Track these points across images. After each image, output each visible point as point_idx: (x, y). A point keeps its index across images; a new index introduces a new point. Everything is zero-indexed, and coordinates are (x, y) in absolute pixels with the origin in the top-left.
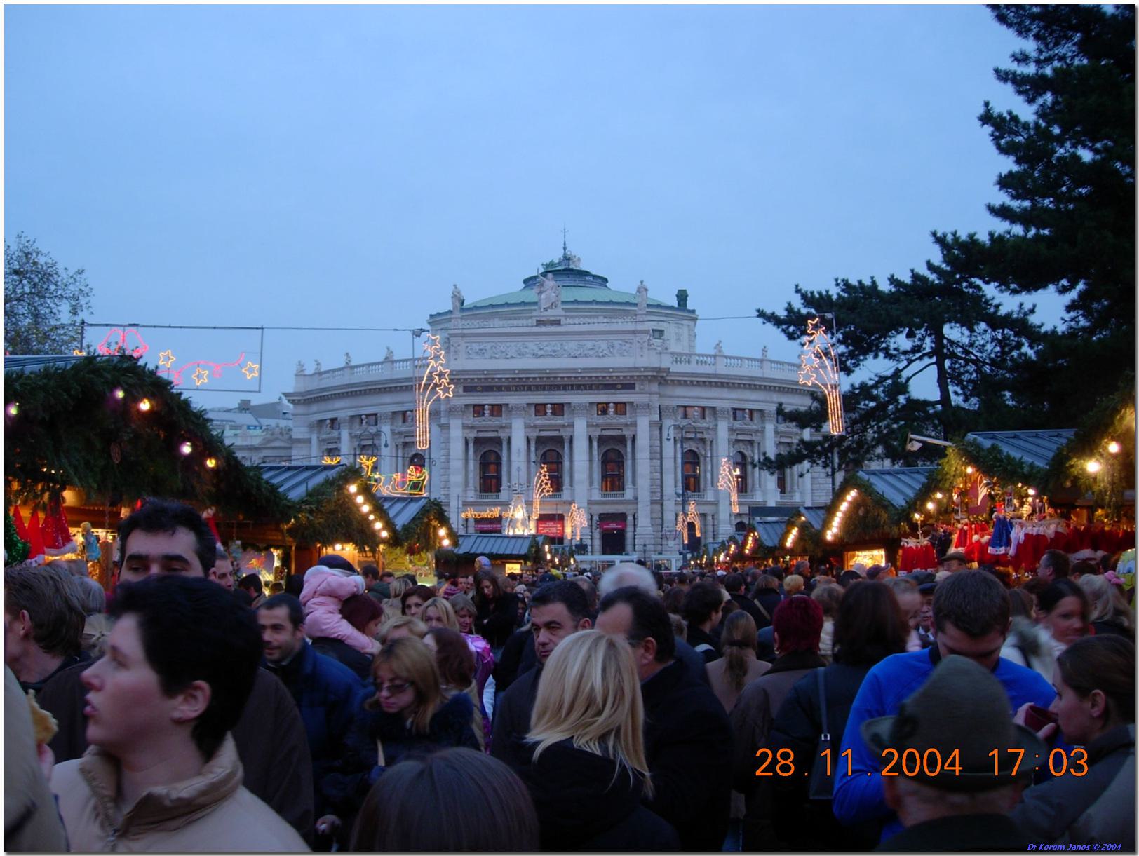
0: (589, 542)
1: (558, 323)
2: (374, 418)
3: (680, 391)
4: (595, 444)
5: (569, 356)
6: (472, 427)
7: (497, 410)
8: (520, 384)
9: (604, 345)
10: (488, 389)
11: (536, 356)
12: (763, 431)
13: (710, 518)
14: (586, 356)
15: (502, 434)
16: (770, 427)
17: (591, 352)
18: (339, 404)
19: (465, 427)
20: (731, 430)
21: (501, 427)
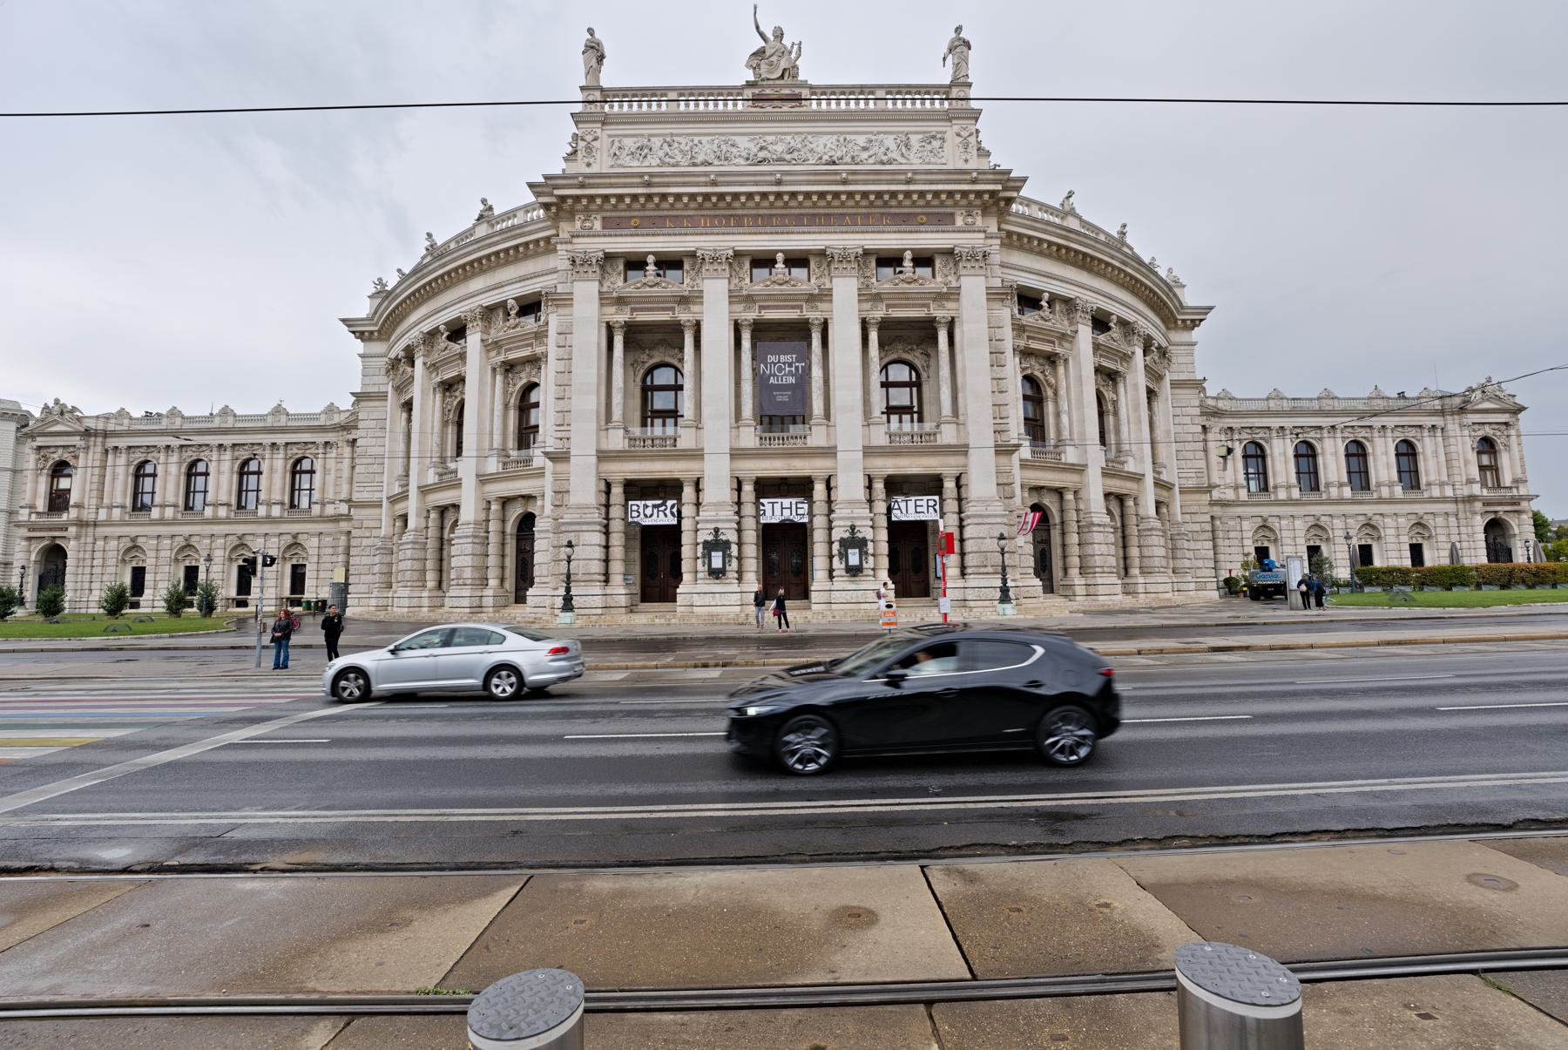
0: (867, 533)
1: (798, 99)
2: (457, 332)
3: (1018, 258)
4: (874, 336)
6: (621, 301)
7: (669, 263)
8: (719, 207)
9: (890, 142)
10: (653, 224)
12: (1127, 358)
13: (1069, 497)
15: (683, 316)
16: (1139, 352)
17: (864, 155)
18: (413, 318)
19: (604, 299)
20: (1097, 347)
21: (684, 300)
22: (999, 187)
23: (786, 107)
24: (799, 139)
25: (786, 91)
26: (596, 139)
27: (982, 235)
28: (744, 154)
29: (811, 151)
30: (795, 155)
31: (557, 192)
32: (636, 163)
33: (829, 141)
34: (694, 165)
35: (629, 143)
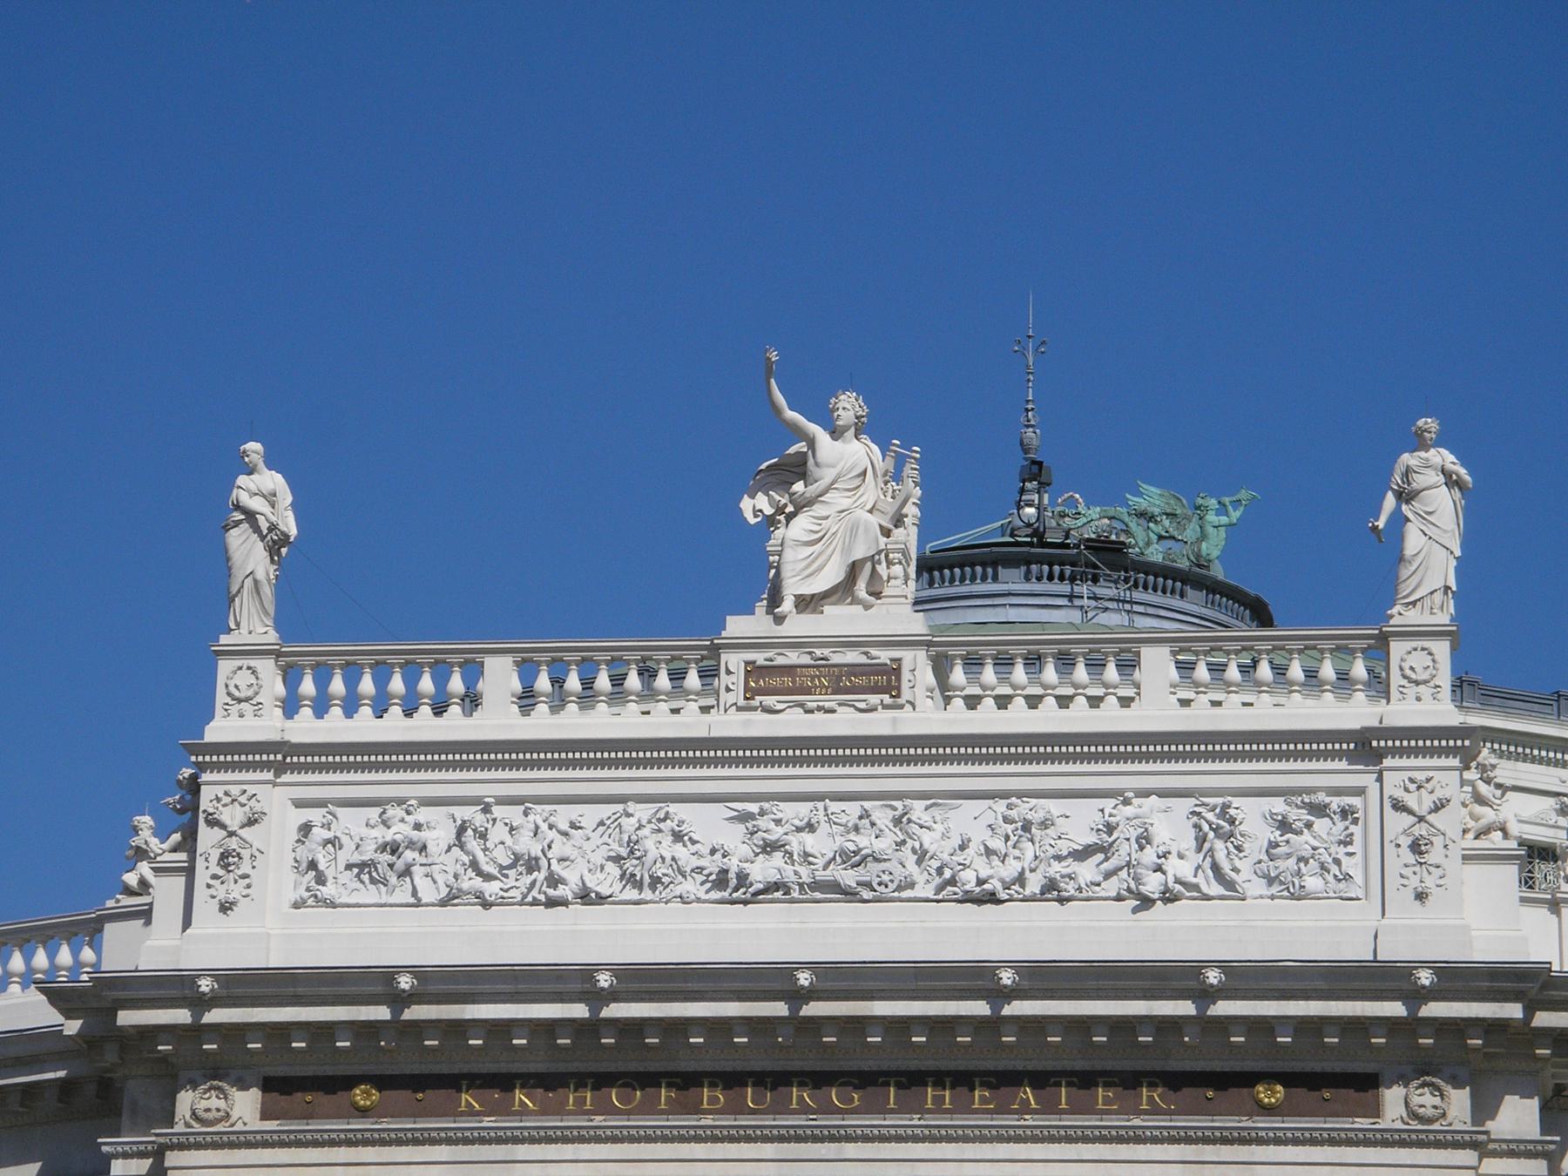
1: (887, 681)
5: (950, 890)
9: (1171, 826)
11: (731, 886)
14: (1051, 889)
17: (1087, 871)
22: (1514, 1011)
23: (846, 720)
24: (882, 816)
25: (853, 657)
26: (251, 822)
27: (1468, 1157)
28: (712, 865)
29: (922, 856)
30: (871, 872)
31: (126, 1018)
32: (371, 894)
33: (973, 821)
34: (552, 903)
35: (359, 830)
